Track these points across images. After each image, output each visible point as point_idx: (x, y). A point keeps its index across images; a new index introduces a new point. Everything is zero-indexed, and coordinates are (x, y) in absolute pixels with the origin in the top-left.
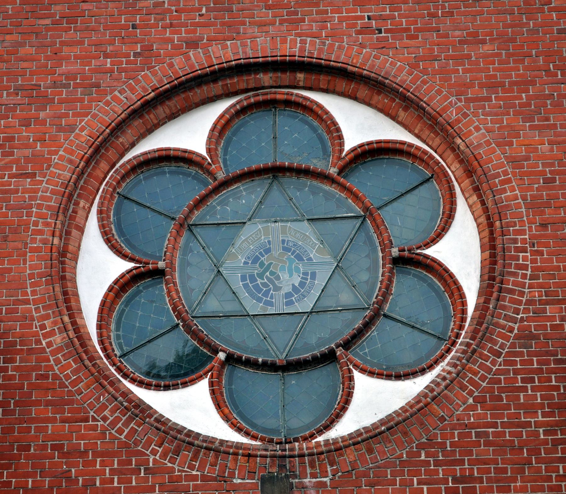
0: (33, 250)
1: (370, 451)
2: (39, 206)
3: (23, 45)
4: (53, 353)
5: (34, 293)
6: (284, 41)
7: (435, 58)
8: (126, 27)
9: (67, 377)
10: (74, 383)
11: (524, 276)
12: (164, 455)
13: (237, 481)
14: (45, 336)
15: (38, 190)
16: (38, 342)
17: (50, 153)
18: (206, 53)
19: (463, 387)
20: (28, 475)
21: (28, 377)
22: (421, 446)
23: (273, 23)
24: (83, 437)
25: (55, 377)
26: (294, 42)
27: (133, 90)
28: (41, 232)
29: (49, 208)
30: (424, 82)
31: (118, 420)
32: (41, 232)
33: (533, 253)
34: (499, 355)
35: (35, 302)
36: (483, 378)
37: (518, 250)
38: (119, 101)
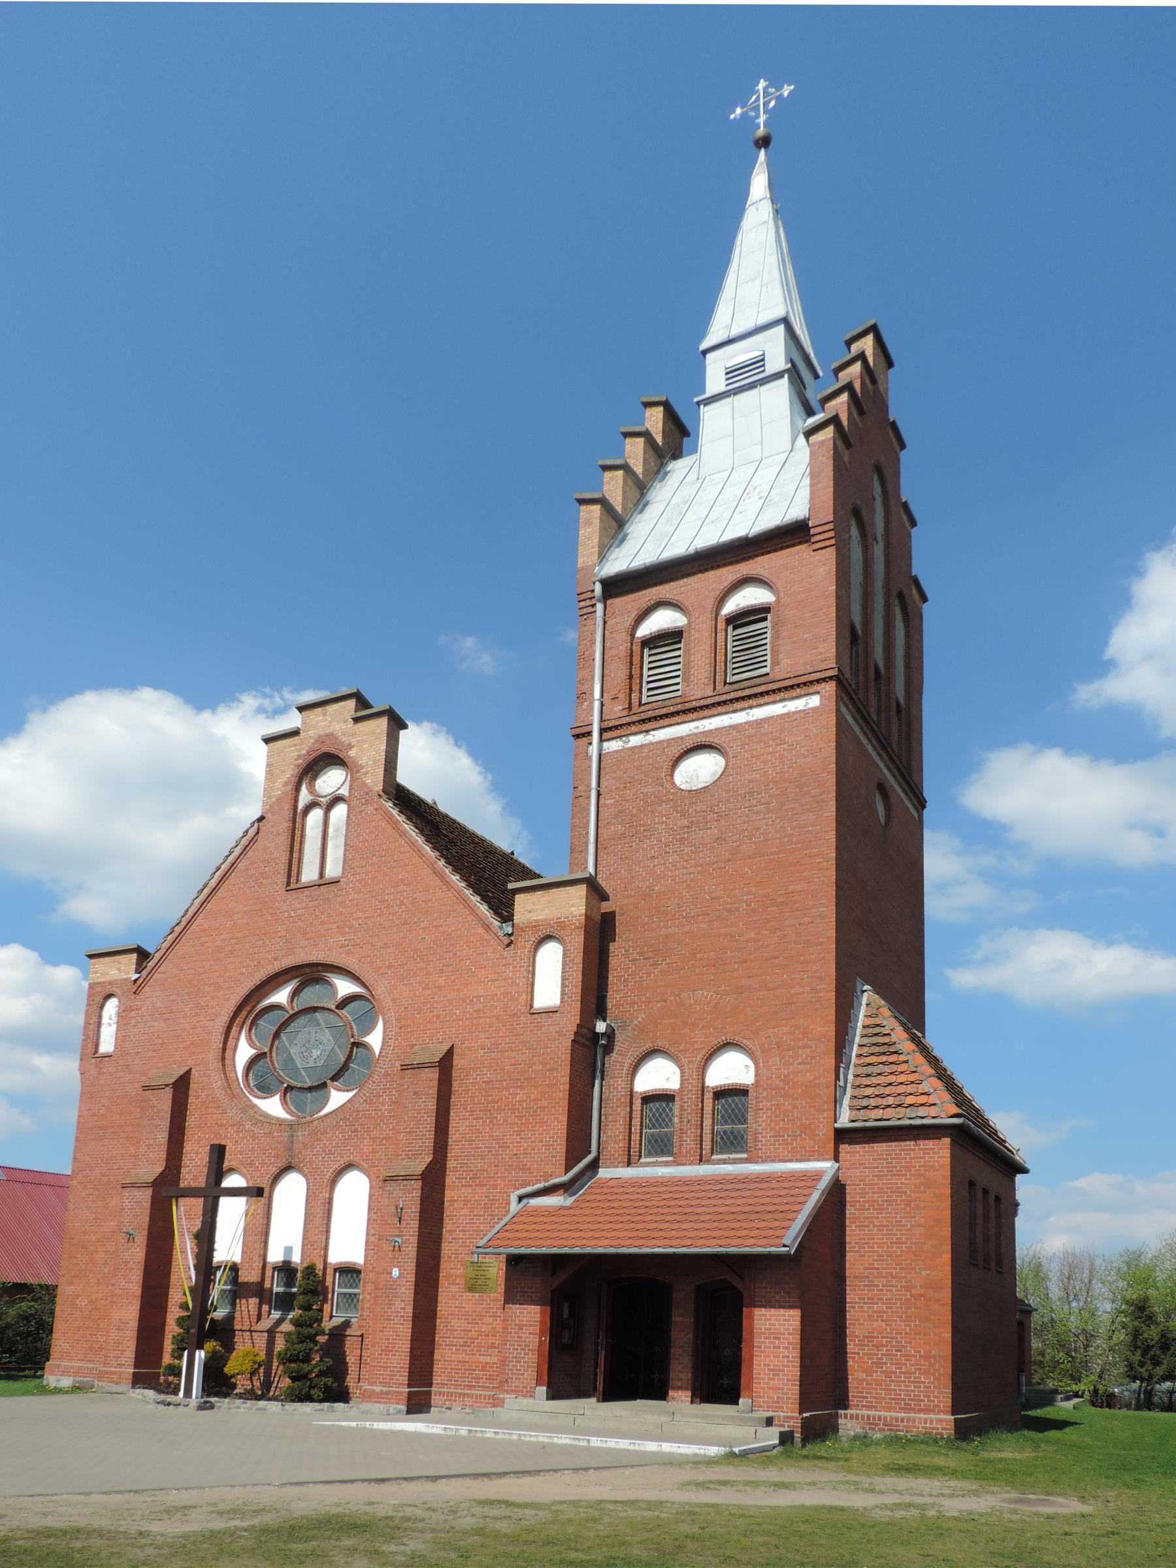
33: (395, 1040)
38: (247, 986)
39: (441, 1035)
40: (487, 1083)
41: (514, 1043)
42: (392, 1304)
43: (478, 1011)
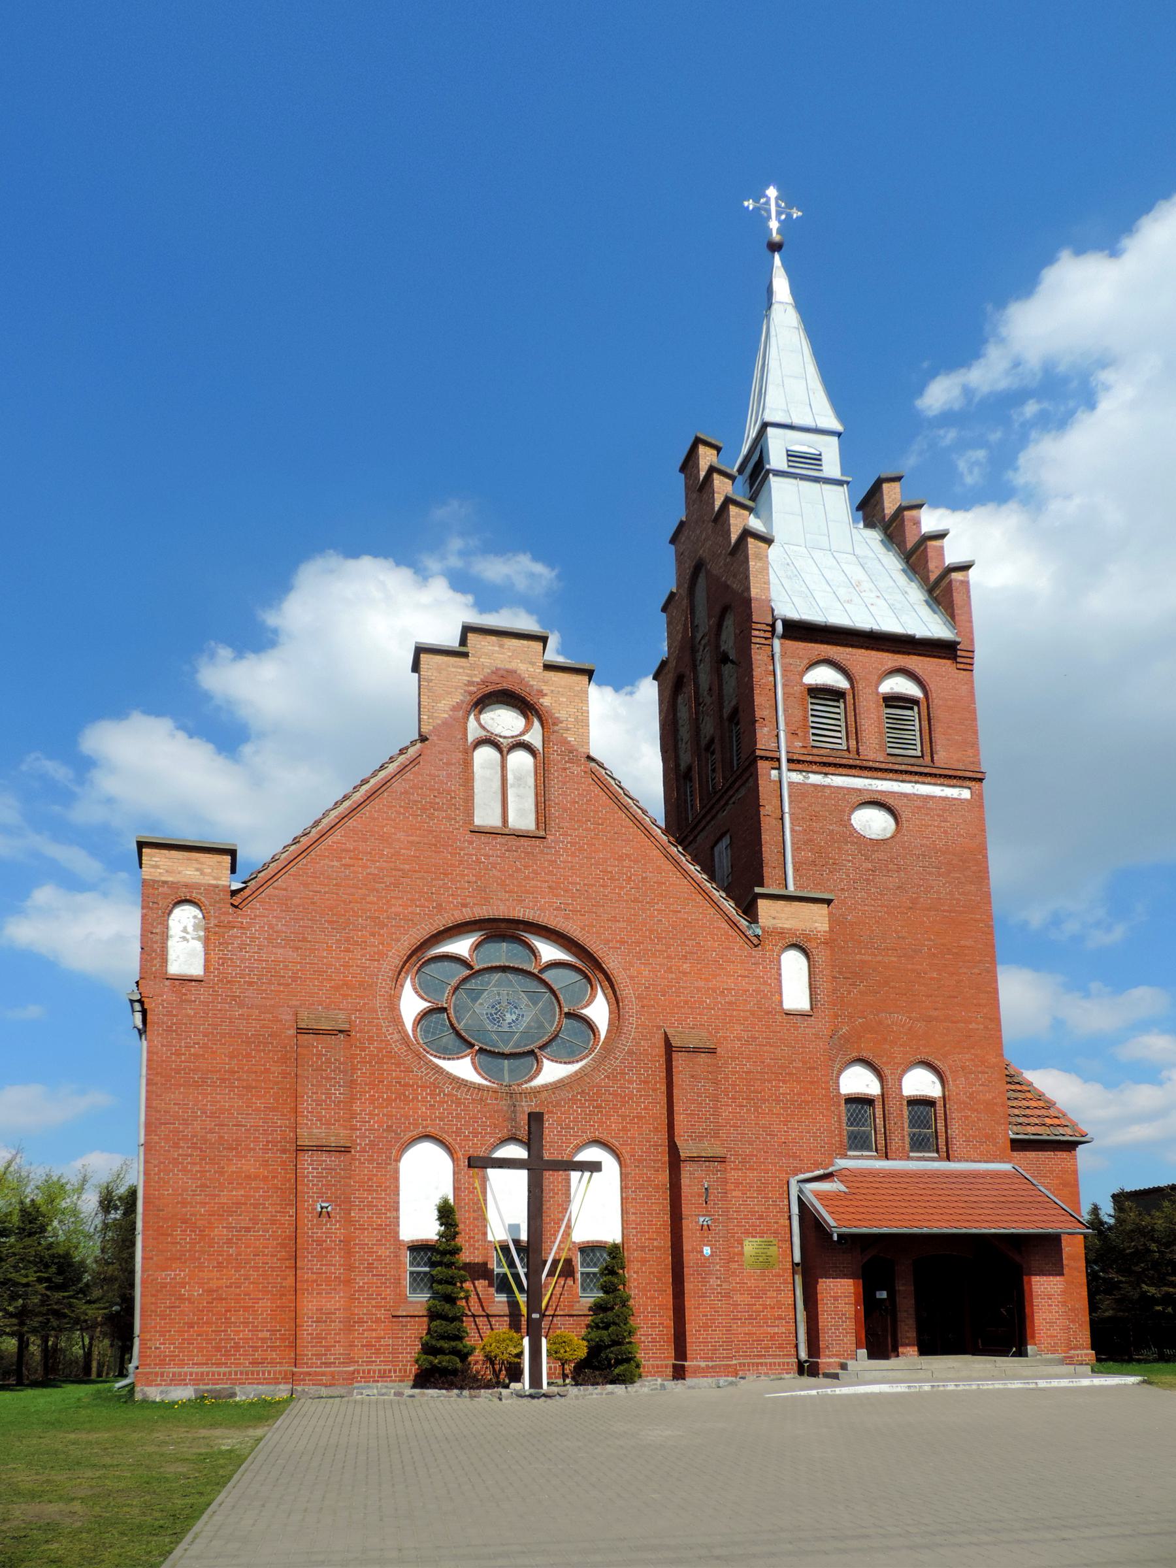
0: (380, 995)
1: (554, 1093)
2: (382, 975)
3: (369, 896)
4: (394, 1042)
5: (382, 1015)
6: (514, 909)
7: (594, 926)
8: (427, 893)
9: (402, 1053)
10: (405, 1056)
11: (632, 1028)
12: (453, 1089)
13: (489, 1101)
14: (389, 1034)
15: (381, 968)
16: (386, 1037)
17: (387, 950)
18: (472, 910)
19: (600, 1071)
20: (383, 1093)
21: (382, 1052)
22: (578, 1093)
23: (508, 900)
24: (411, 1079)
25: (395, 1052)
26: (519, 911)
27: (432, 925)
28: (384, 987)
29: (388, 976)
30: (587, 937)
31: (428, 1073)
32: (384, 987)
34: (617, 1059)
35: (383, 1019)
36: (609, 1068)
37: (629, 1016)
38: (425, 929)
39: (691, 1021)
40: (748, 1073)
41: (772, 1039)
42: (707, 1282)
43: (730, 1003)
